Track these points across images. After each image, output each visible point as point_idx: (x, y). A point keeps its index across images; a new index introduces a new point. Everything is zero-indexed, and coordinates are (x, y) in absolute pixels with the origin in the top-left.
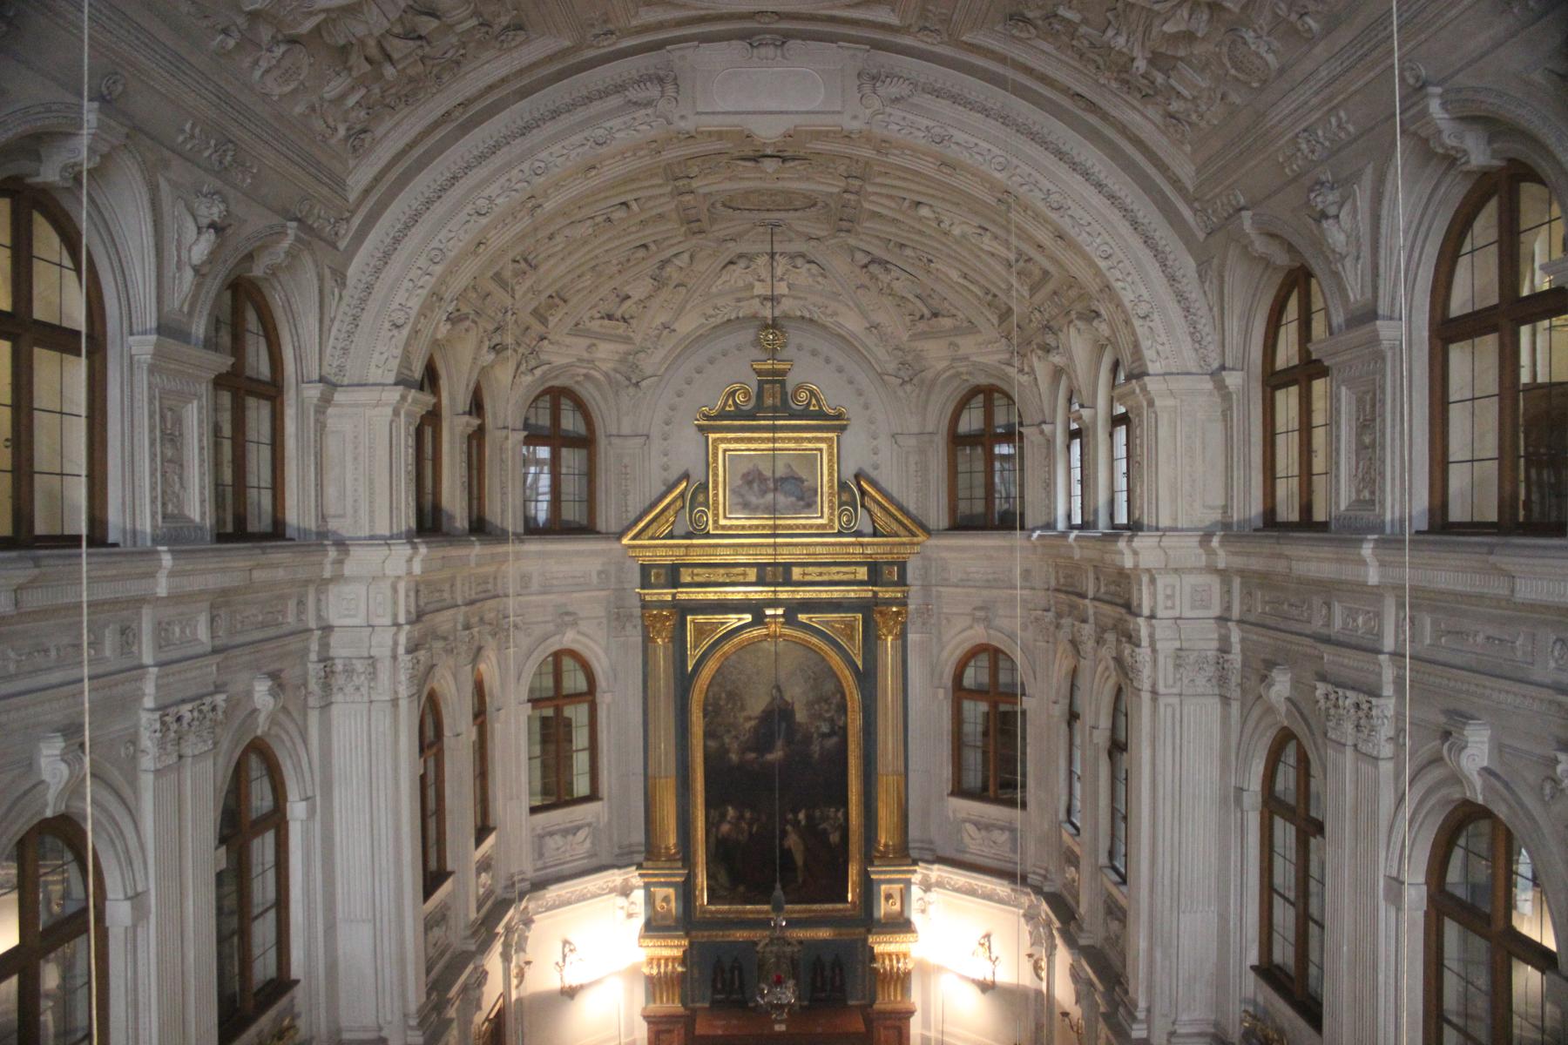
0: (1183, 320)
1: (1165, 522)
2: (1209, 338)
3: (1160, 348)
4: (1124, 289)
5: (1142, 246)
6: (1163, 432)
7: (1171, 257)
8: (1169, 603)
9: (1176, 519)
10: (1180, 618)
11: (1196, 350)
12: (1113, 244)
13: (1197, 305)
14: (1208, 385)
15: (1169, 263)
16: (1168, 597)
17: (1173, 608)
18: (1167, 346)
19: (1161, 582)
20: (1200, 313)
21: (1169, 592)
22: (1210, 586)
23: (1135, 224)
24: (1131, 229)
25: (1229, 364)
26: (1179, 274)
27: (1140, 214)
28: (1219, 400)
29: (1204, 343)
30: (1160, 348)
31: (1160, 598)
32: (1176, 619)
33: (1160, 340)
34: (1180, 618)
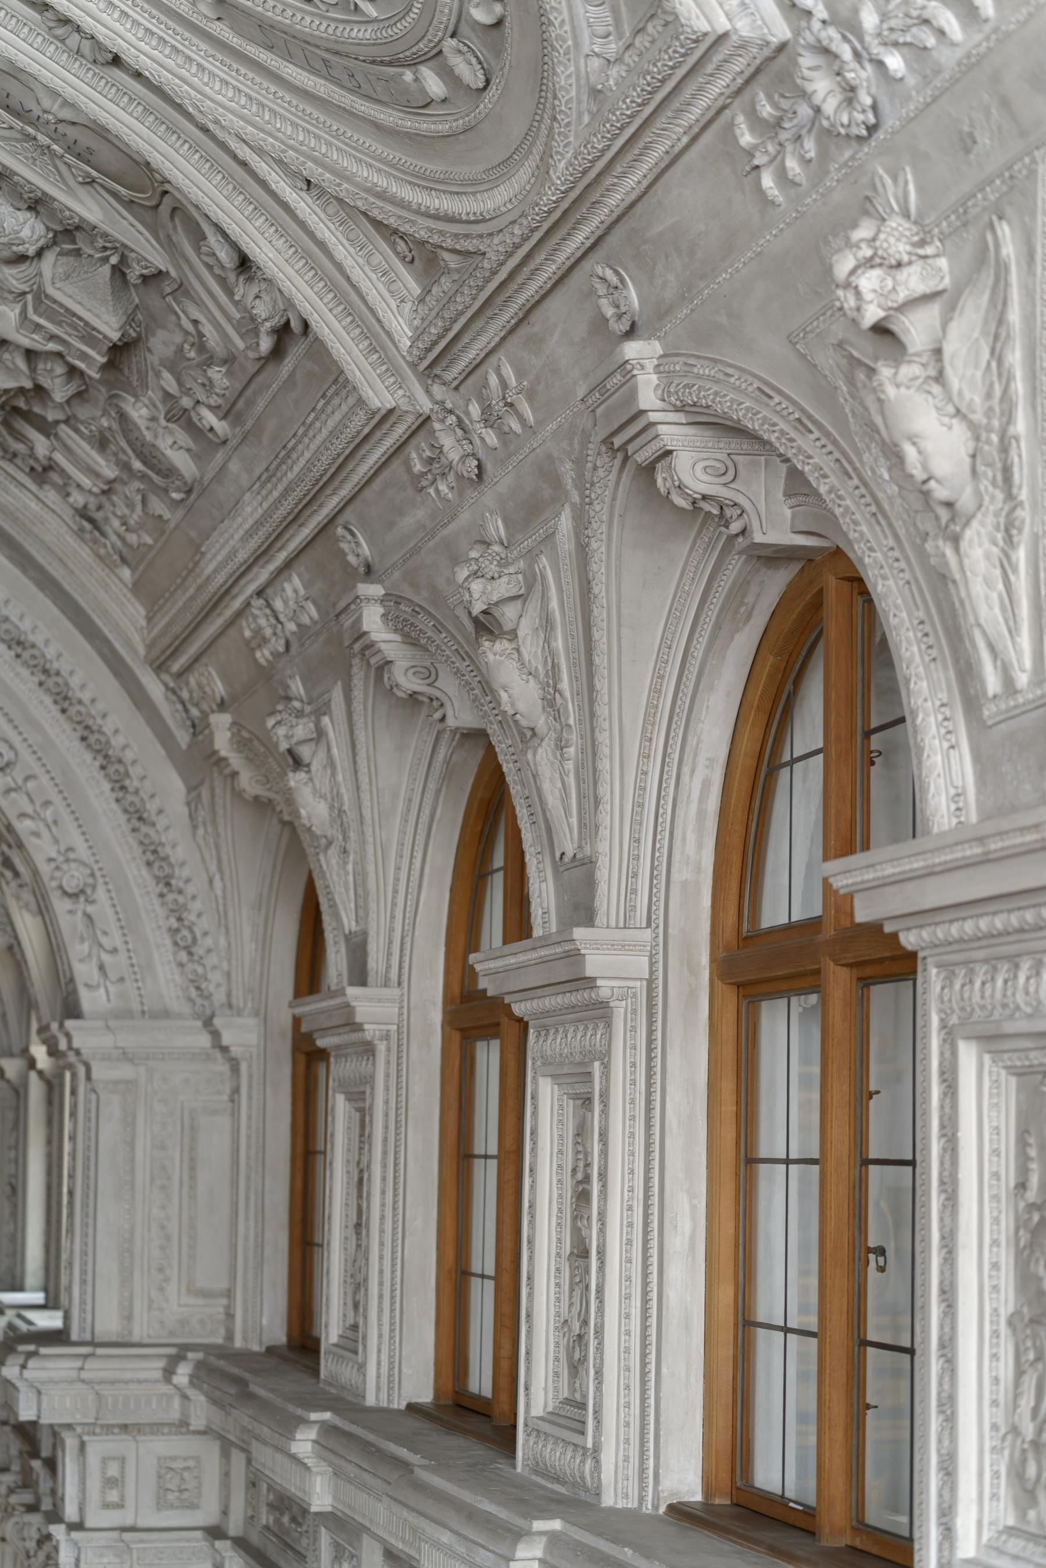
0: (156, 902)
1: (108, 1324)
2: (209, 942)
3: (106, 958)
4: (37, 834)
5: (77, 745)
6: (109, 1132)
7: (135, 771)
8: (113, 1496)
9: (129, 1318)
10: (133, 1529)
11: (181, 965)
12: (16, 740)
13: (186, 873)
14: (204, 1040)
15: (132, 784)
16: (110, 1483)
17: (120, 1506)
18: (122, 956)
19: (96, 1449)
20: (190, 889)
21: (113, 1471)
22: (197, 1459)
23: (63, 700)
24: (55, 710)
25: (238, 999)
26: (152, 806)
27: (75, 682)
28: (222, 1067)
29: (199, 951)
30: (106, 958)
31: (94, 1484)
32: (124, 1529)
33: (104, 940)
34: (133, 1529)
